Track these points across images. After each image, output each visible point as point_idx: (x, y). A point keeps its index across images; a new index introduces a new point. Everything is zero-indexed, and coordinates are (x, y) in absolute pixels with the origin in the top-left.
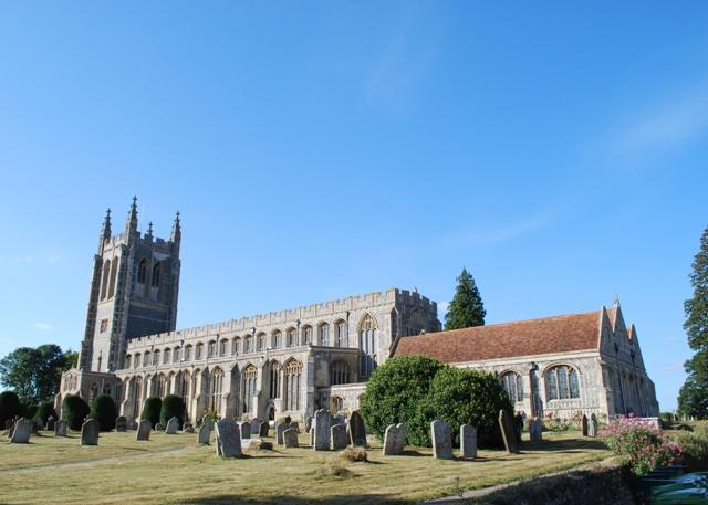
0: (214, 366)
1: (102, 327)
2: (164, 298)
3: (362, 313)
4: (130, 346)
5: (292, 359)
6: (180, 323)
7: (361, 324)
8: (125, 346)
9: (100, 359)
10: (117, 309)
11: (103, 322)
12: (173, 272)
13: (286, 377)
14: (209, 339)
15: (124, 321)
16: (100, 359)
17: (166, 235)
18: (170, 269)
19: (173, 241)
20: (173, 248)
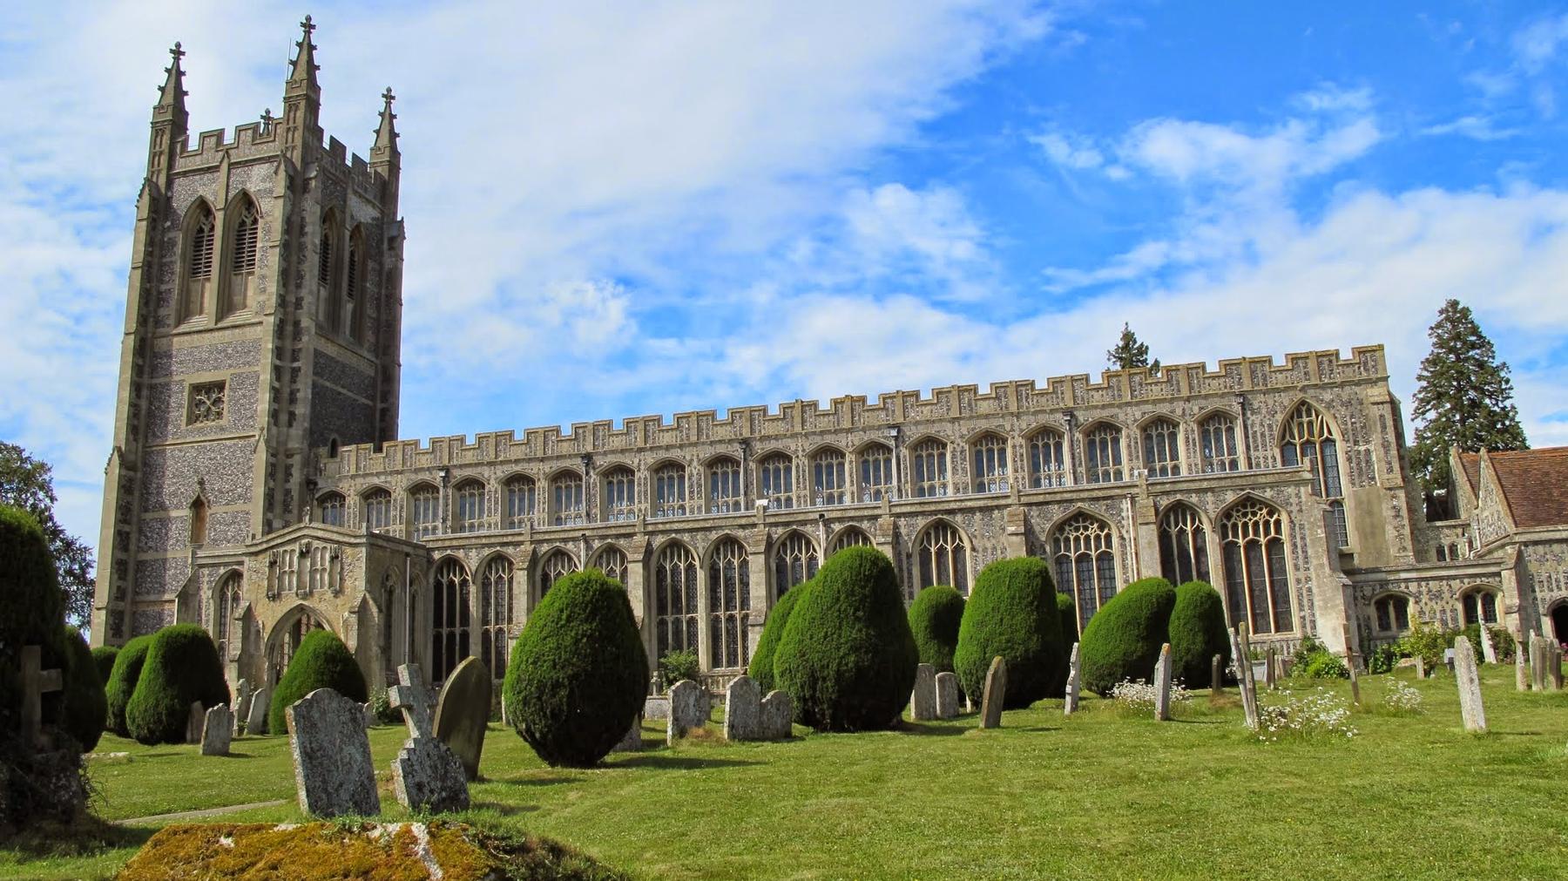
0: (921, 522)
1: (195, 404)
2: (370, 336)
3: (1288, 400)
4: (331, 466)
5: (1248, 503)
6: (420, 418)
7: (1286, 429)
8: (312, 465)
9: (198, 505)
10: (279, 352)
11: (197, 388)
12: (388, 262)
13: (1229, 551)
14: (708, 452)
15: (305, 392)
16: (198, 505)
17: (360, 145)
18: (381, 254)
19: (385, 174)
20: (386, 191)
